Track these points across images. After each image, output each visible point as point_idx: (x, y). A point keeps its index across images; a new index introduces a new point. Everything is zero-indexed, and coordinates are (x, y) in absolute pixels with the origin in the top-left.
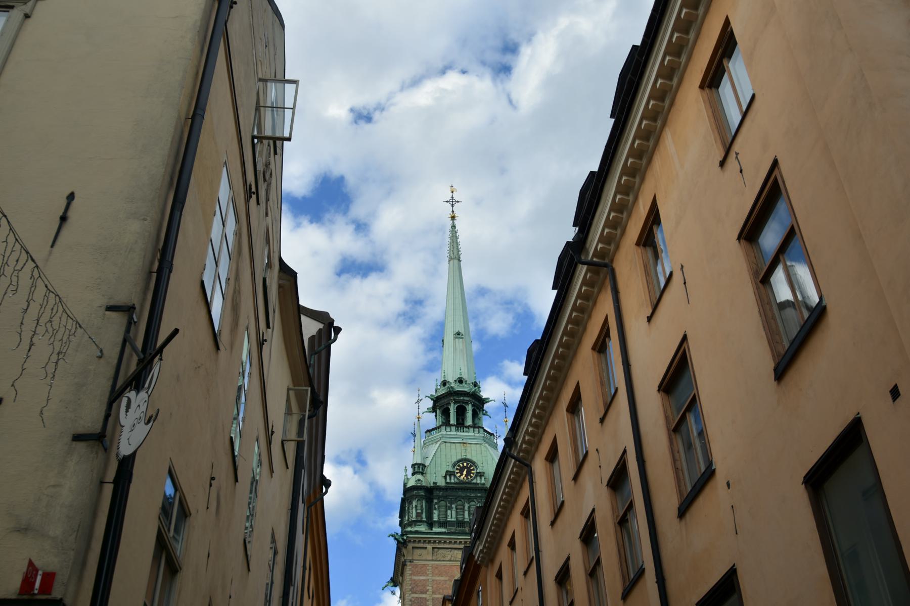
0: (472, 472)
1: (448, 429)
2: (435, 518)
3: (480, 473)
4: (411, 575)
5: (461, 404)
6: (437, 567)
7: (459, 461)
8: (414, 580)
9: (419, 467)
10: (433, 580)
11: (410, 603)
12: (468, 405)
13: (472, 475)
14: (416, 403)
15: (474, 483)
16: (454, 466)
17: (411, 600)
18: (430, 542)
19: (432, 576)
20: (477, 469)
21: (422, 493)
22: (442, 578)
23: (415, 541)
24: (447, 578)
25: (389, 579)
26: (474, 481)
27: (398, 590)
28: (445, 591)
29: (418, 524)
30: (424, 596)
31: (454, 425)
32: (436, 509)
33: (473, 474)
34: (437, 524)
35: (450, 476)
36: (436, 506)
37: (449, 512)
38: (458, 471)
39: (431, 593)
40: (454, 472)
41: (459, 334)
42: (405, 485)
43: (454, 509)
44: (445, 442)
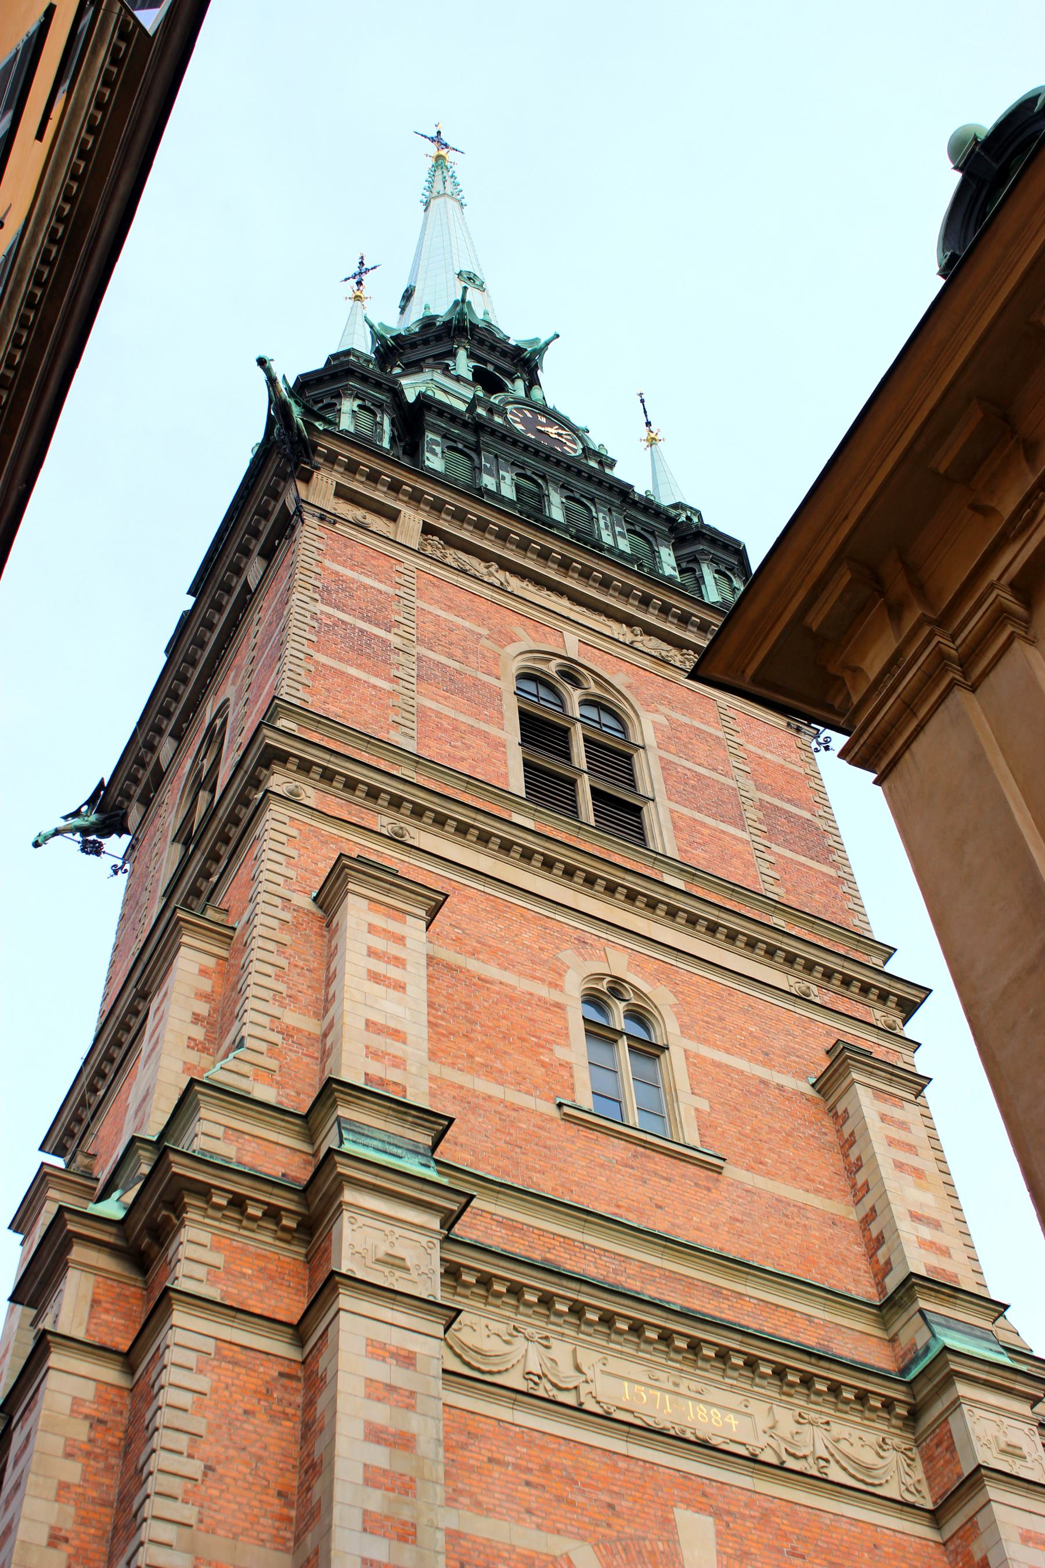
2: (435, 462)
5: (490, 368)
8: (337, 573)
12: (513, 381)
14: (346, 279)
18: (416, 498)
19: (420, 598)
22: (467, 624)
24: (485, 632)
27: (116, 845)
28: (470, 656)
30: (382, 633)
36: (438, 449)
38: (518, 420)
41: (470, 279)
43: (508, 480)
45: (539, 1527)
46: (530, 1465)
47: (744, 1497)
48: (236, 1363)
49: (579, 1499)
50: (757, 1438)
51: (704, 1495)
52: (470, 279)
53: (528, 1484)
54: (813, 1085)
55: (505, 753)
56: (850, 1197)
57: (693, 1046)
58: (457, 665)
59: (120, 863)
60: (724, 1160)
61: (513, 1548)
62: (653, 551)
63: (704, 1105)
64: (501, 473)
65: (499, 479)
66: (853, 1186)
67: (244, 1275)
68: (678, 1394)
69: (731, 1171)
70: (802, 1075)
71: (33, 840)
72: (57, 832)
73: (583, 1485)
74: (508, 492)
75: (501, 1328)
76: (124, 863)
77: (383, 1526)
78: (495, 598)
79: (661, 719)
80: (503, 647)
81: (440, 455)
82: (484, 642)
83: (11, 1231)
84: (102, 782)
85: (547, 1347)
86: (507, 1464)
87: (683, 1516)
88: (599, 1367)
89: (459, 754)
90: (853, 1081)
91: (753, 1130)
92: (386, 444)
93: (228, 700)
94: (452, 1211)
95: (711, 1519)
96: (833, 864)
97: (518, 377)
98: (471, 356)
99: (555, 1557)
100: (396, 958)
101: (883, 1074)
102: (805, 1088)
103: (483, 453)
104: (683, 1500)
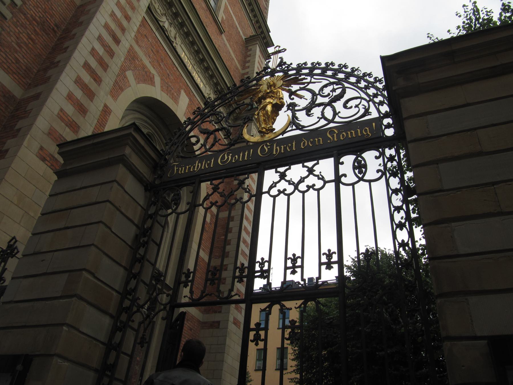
45: (150, 62)
46: (154, 47)
47: (197, 102)
49: (162, 66)
50: (205, 93)
51: (189, 93)
53: (152, 50)
54: (245, 39)
56: (242, 68)
57: (227, 4)
60: (224, 32)
61: (141, 60)
63: (224, 18)
66: (244, 65)
68: (194, 67)
69: (223, 35)
70: (244, 35)
73: (165, 64)
75: (162, 11)
77: (122, 9)
85: (171, 27)
86: (149, 41)
87: (183, 92)
88: (180, 43)
90: (257, 44)
91: (231, 33)
95: (188, 100)
96: (266, 4)
99: (151, 72)
101: (263, 48)
102: (244, 38)
104: (184, 90)
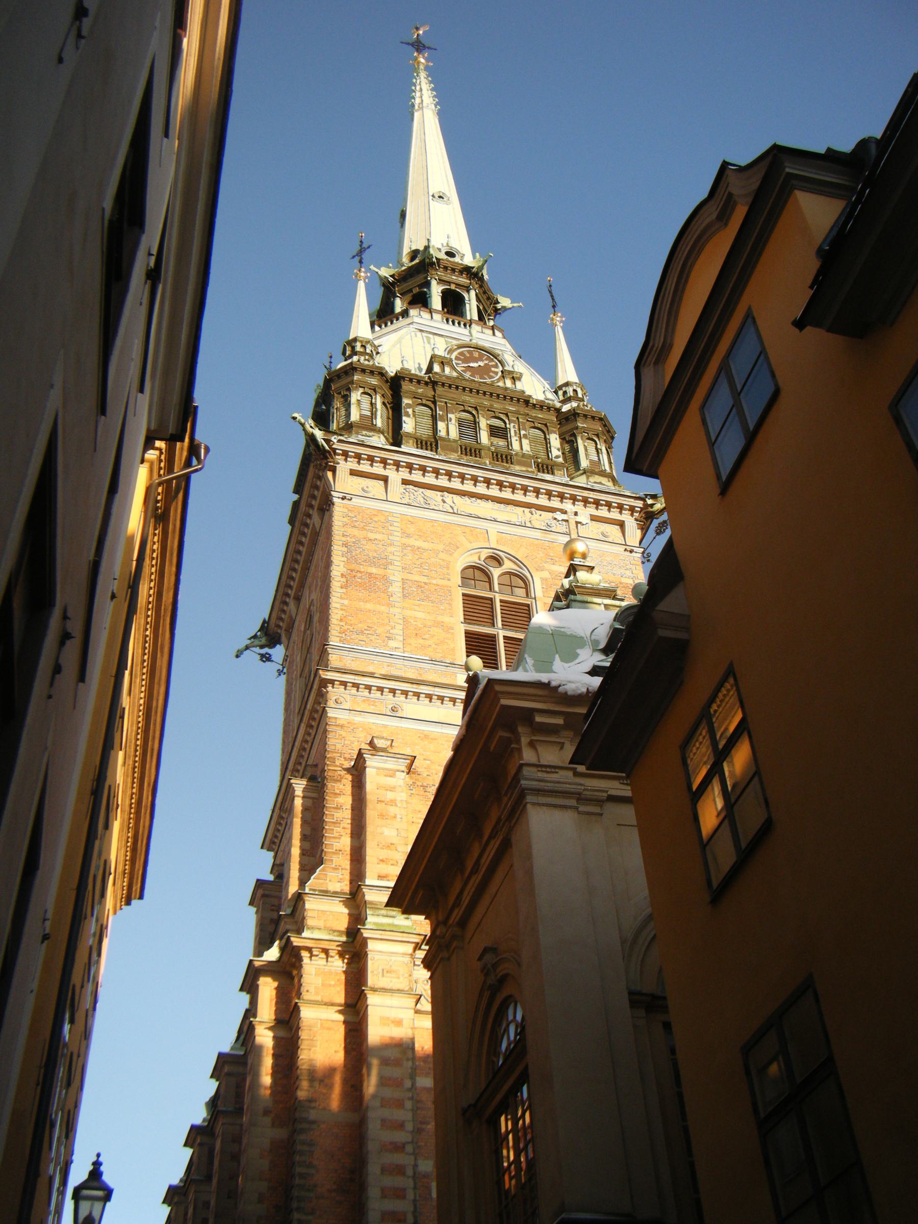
0: (493, 369)
1: (425, 315)
2: (408, 425)
3: (510, 372)
4: (345, 525)
5: (453, 287)
6: (412, 521)
7: (460, 347)
9: (364, 346)
10: (405, 546)
11: (344, 580)
12: (468, 291)
13: (491, 374)
15: (498, 386)
16: (451, 351)
17: (342, 575)
20: (503, 365)
21: (374, 381)
23: (345, 497)
24: (441, 547)
25: (255, 627)
26: (501, 384)
27: (278, 652)
29: (364, 432)
31: (437, 312)
32: (408, 415)
33: (496, 373)
34: (411, 441)
35: (442, 364)
36: (410, 411)
37: (441, 425)
39: (400, 569)
40: (451, 360)
41: (440, 197)
42: (329, 369)
43: (453, 421)
44: (421, 331)
48: (329, 1029)
52: (440, 197)
55: (453, 634)
58: (424, 579)
59: (281, 667)
62: (545, 438)
64: (450, 415)
65: (447, 420)
67: (330, 985)
71: (235, 654)
72: (247, 648)
74: (454, 433)
76: (283, 668)
78: (447, 519)
79: (546, 574)
80: (451, 555)
81: (411, 416)
82: (442, 556)
83: (264, 851)
84: (264, 622)
89: (427, 643)
92: (379, 422)
93: (313, 600)
94: (418, 943)
97: (471, 289)
98: (441, 281)
100: (392, 801)
103: (438, 403)
